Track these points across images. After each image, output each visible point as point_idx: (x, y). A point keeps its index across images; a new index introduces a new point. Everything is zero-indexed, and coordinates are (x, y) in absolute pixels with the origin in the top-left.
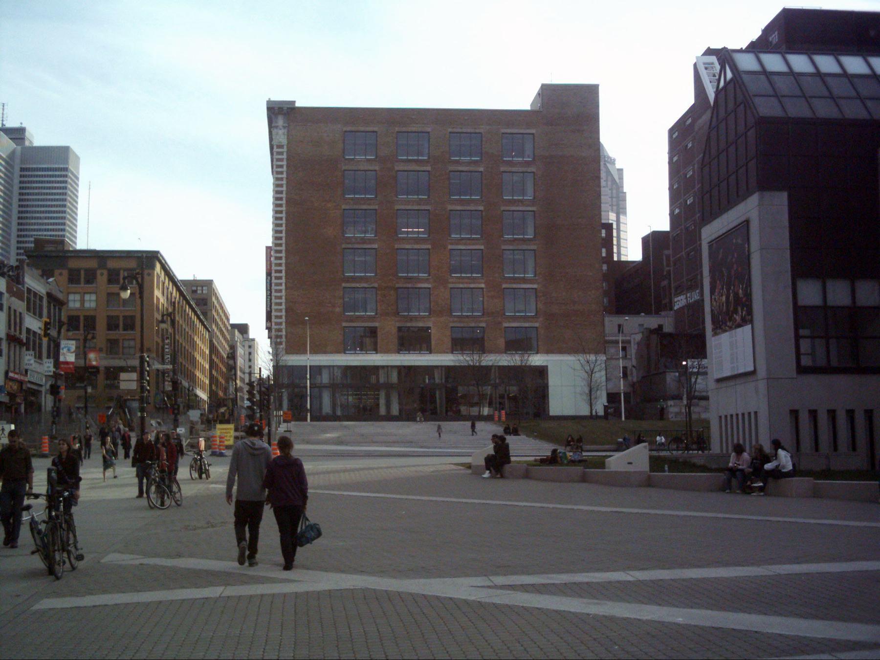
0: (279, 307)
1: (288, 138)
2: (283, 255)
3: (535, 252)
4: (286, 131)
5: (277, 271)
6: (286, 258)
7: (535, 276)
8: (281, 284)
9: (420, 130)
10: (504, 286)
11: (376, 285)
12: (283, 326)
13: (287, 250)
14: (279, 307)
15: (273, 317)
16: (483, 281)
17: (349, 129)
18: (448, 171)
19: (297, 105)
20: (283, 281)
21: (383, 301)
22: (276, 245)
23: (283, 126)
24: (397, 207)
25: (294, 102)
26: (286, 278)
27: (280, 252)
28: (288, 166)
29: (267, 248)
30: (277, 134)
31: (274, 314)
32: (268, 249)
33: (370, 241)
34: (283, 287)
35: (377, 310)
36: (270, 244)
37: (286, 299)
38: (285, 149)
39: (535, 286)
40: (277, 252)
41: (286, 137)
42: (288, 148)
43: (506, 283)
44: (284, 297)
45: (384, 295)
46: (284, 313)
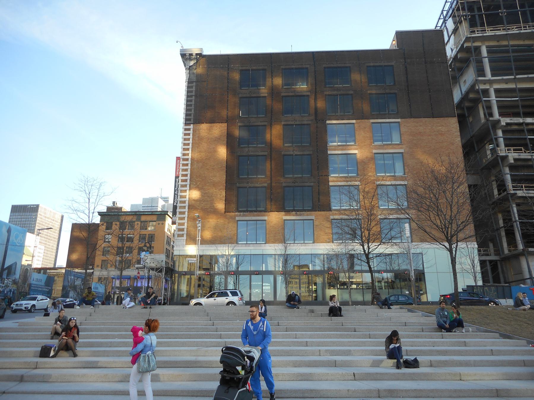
3: (403, 156)
5: (183, 175)
7: (405, 174)
15: (178, 213)
19: (205, 53)
22: (184, 155)
25: (201, 49)
29: (178, 158)
31: (178, 210)
32: (178, 158)
36: (180, 155)
40: (184, 160)
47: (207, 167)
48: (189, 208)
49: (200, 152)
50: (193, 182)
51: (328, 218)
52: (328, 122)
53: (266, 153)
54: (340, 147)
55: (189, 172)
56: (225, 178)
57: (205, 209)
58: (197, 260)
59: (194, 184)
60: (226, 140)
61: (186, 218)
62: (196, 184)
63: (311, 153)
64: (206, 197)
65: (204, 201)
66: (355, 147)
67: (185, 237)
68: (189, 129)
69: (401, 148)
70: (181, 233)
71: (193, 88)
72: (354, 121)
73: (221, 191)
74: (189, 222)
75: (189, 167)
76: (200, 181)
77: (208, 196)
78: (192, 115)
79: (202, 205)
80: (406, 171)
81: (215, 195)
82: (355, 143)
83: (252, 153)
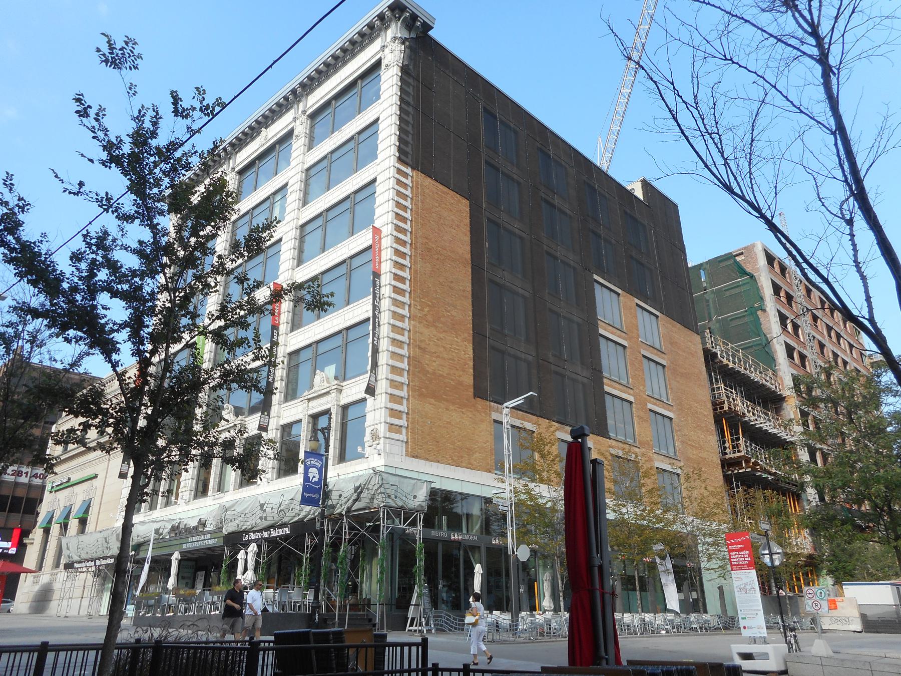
16: (631, 392)
47: (441, 281)
49: (427, 238)
52: (596, 277)
53: (527, 294)
56: (471, 318)
60: (469, 234)
63: (580, 321)
68: (405, 175)
69: (663, 358)
72: (619, 291)
76: (429, 306)
77: (444, 347)
81: (455, 349)
83: (508, 284)
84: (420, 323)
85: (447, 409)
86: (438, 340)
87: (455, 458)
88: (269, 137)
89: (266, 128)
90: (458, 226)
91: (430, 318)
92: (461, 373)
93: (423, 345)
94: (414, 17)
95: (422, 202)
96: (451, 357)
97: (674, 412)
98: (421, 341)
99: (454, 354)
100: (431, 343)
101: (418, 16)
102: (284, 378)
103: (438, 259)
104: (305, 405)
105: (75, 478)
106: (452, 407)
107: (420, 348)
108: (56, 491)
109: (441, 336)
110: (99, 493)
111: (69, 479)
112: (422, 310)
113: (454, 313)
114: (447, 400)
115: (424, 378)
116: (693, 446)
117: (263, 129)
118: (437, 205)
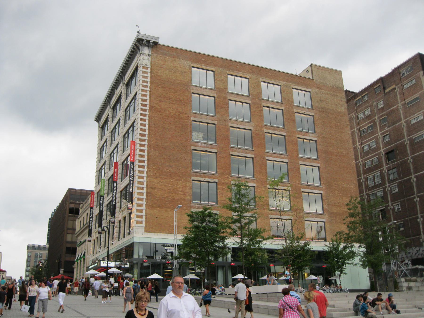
0: (141, 191)
1: (151, 63)
2: (146, 148)
4: (150, 58)
6: (148, 151)
7: (320, 185)
8: (143, 172)
9: (242, 76)
10: (303, 190)
11: (217, 181)
12: (144, 207)
13: (149, 145)
14: (141, 191)
16: (289, 185)
17: (195, 65)
18: (262, 106)
19: (160, 42)
20: (145, 169)
21: (222, 194)
23: (148, 55)
24: (230, 125)
26: (148, 167)
27: (144, 146)
28: (151, 82)
30: (144, 59)
33: (212, 146)
34: (145, 175)
35: (217, 200)
37: (147, 185)
38: (149, 70)
39: (321, 192)
41: (150, 62)
42: (151, 69)
43: (304, 188)
44: (145, 183)
45: (223, 189)
46: (144, 196)
48: (147, 196)
49: (156, 140)
50: (150, 170)
51: (267, 217)
54: (276, 155)
55: (146, 159)
57: (163, 197)
58: (176, 249)
59: (152, 171)
61: (144, 206)
62: (154, 172)
64: (164, 186)
65: (161, 190)
66: (286, 156)
67: (144, 225)
69: (318, 163)
70: (140, 219)
71: (148, 74)
73: (177, 181)
74: (148, 210)
75: (146, 153)
76: (157, 169)
77: (165, 185)
78: (148, 101)
79: (160, 193)
80: (322, 183)
81: (171, 185)
82: (286, 153)
84: (152, 177)
85: (166, 211)
86: (161, 183)
87: (170, 231)
88: (118, 92)
89: (117, 89)
90: (174, 130)
91: (157, 174)
92: (174, 195)
93: (154, 187)
94: (148, 41)
95: (154, 124)
96: (169, 189)
97: (323, 190)
98: (153, 185)
99: (170, 187)
100: (158, 185)
101: (150, 41)
102: (119, 201)
103: (162, 148)
104: (121, 213)
105: (82, 241)
106: (168, 210)
107: (152, 188)
108: (79, 246)
109: (164, 181)
110: (87, 248)
111: (81, 242)
112: (154, 172)
113: (171, 169)
114: (166, 207)
115: (154, 200)
116: (338, 206)
117: (116, 90)
118: (163, 123)
